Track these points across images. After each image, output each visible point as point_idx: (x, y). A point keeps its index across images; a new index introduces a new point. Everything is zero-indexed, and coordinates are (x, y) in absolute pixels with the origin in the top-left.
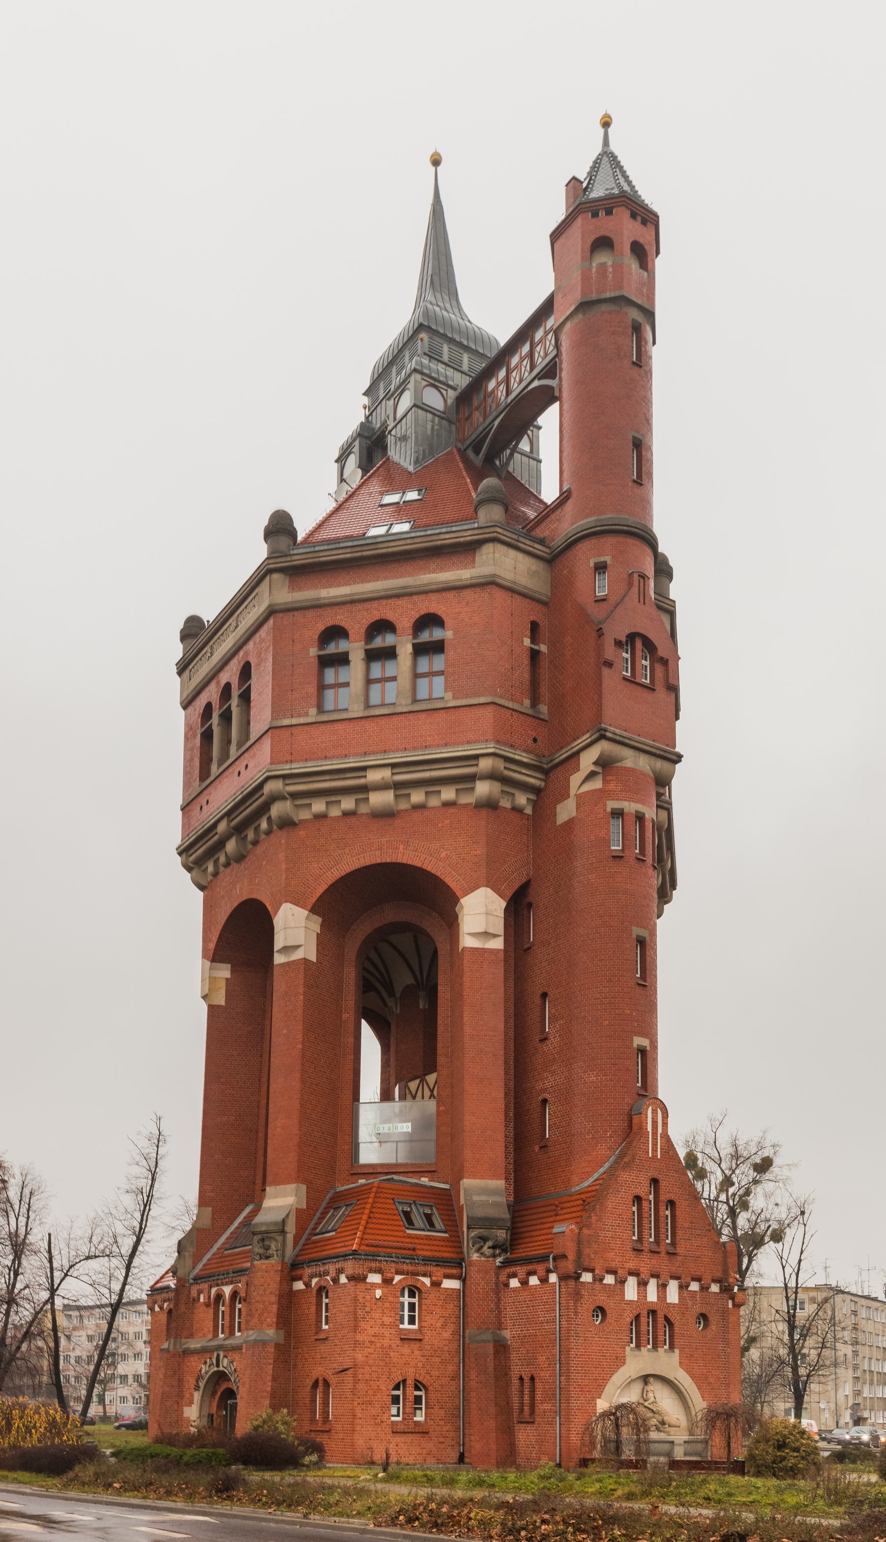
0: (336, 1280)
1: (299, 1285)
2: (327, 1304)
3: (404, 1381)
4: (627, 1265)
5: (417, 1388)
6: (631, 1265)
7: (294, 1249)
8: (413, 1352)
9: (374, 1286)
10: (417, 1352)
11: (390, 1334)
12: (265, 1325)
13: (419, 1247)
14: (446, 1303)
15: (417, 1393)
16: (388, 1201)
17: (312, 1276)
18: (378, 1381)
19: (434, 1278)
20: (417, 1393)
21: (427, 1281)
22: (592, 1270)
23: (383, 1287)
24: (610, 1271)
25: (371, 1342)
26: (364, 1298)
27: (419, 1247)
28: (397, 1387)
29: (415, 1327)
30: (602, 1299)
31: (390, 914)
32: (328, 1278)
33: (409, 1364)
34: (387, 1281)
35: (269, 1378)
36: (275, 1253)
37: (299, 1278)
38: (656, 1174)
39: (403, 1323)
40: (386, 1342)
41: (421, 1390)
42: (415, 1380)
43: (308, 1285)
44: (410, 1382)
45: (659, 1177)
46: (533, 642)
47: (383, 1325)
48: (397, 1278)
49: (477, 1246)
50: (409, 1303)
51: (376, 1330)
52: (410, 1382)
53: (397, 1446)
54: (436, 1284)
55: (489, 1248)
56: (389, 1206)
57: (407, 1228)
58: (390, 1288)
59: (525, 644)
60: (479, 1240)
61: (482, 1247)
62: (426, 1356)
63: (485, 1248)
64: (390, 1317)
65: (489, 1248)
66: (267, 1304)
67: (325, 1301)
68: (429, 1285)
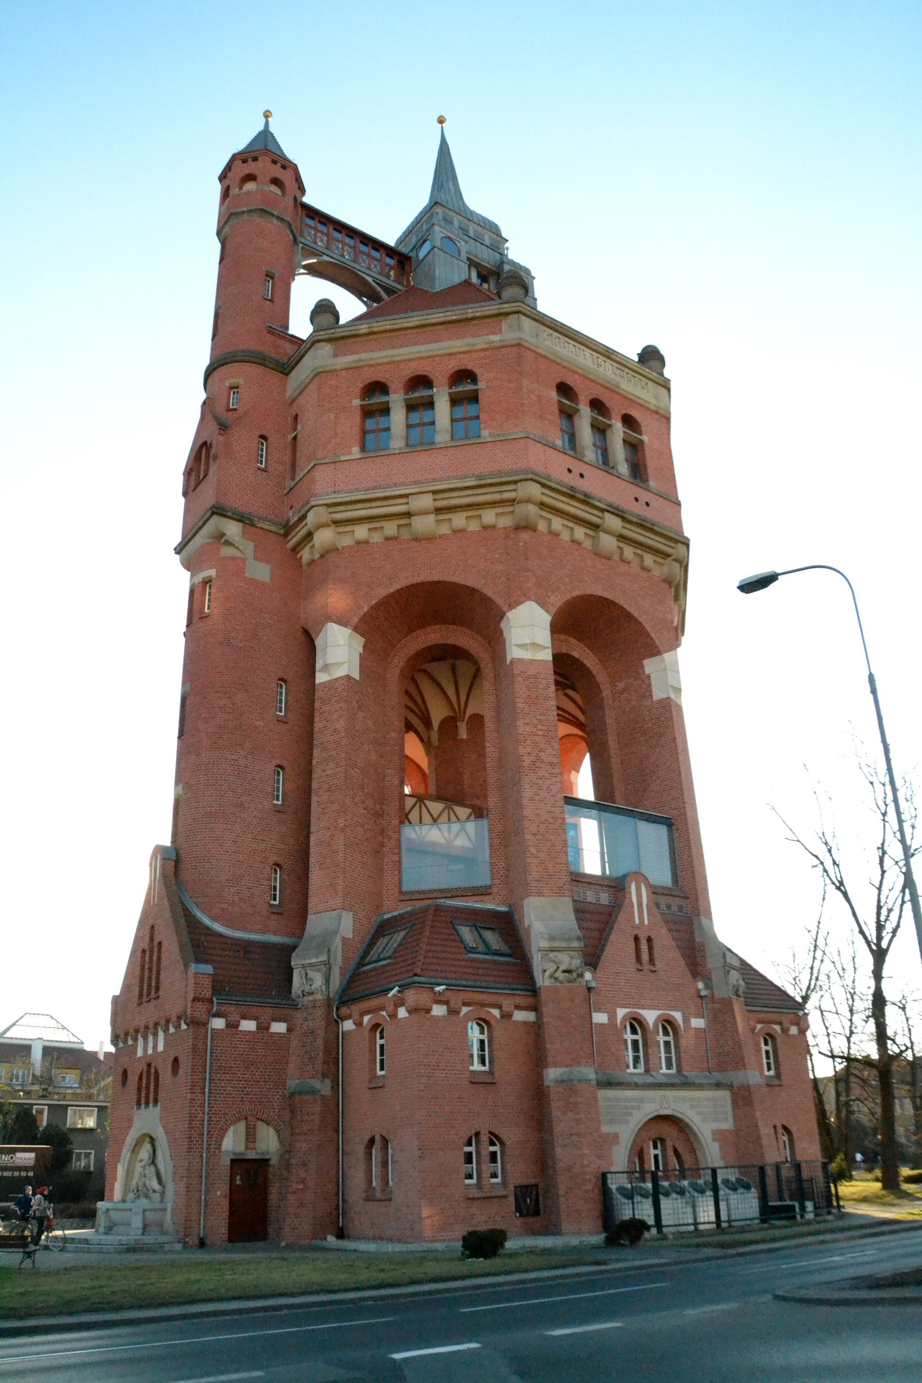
0: (393, 1016)
1: (348, 1025)
2: (382, 1046)
3: (477, 1134)
5: (492, 1143)
15: (492, 1149)
17: (362, 1014)
20: (492, 1149)
21: (496, 1012)
28: (469, 1144)
29: (486, 1068)
31: (434, 636)
32: (384, 1013)
37: (348, 1017)
39: (472, 1064)
41: (495, 1145)
42: (490, 1133)
43: (359, 1024)
44: (484, 1138)
52: (484, 1138)
54: (507, 1016)
67: (380, 1042)
68: (498, 1016)
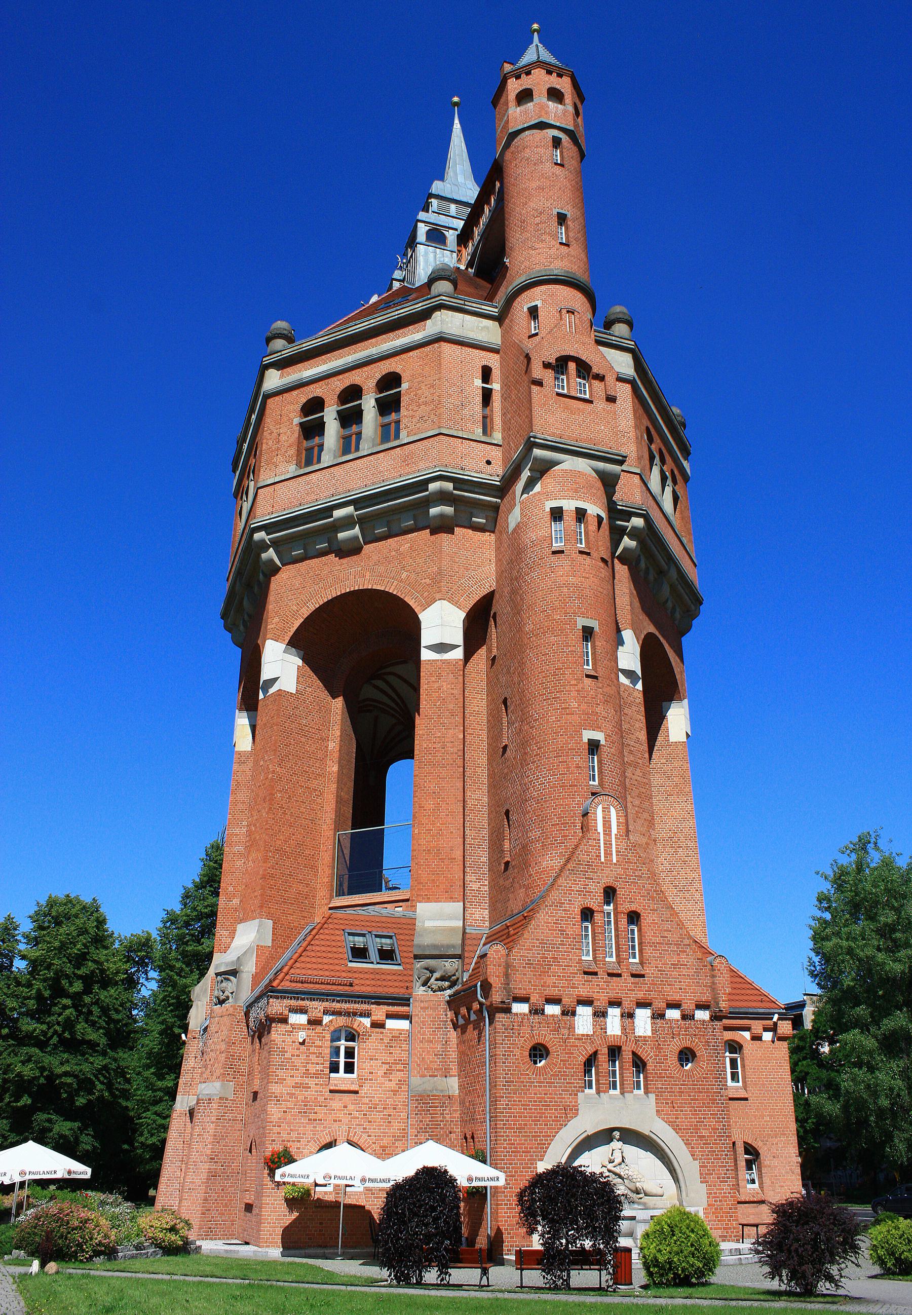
4: (576, 992)
6: (584, 992)
7: (252, 991)
8: (345, 1107)
9: (298, 1027)
10: (351, 1107)
11: (316, 1084)
12: (214, 1078)
13: (357, 982)
14: (392, 1047)
16: (337, 932)
18: (300, 1141)
19: (374, 1018)
22: (524, 1000)
23: (308, 1029)
24: (551, 1001)
25: (291, 1095)
26: (284, 1041)
27: (357, 982)
30: (546, 1036)
33: (340, 1121)
34: (314, 1022)
35: (210, 1139)
36: (230, 995)
38: (610, 881)
40: (310, 1094)
45: (617, 885)
46: (483, 382)
47: (307, 1073)
48: (326, 1019)
49: (423, 978)
50: (346, 1048)
51: (298, 1080)
53: (321, 1223)
54: (378, 1025)
55: (437, 980)
56: (338, 938)
57: (351, 961)
58: (319, 1029)
59: (476, 384)
60: (426, 971)
61: (429, 979)
62: (362, 1111)
63: (432, 980)
64: (317, 1064)
65: (437, 980)
66: (218, 1053)
68: (369, 1025)
